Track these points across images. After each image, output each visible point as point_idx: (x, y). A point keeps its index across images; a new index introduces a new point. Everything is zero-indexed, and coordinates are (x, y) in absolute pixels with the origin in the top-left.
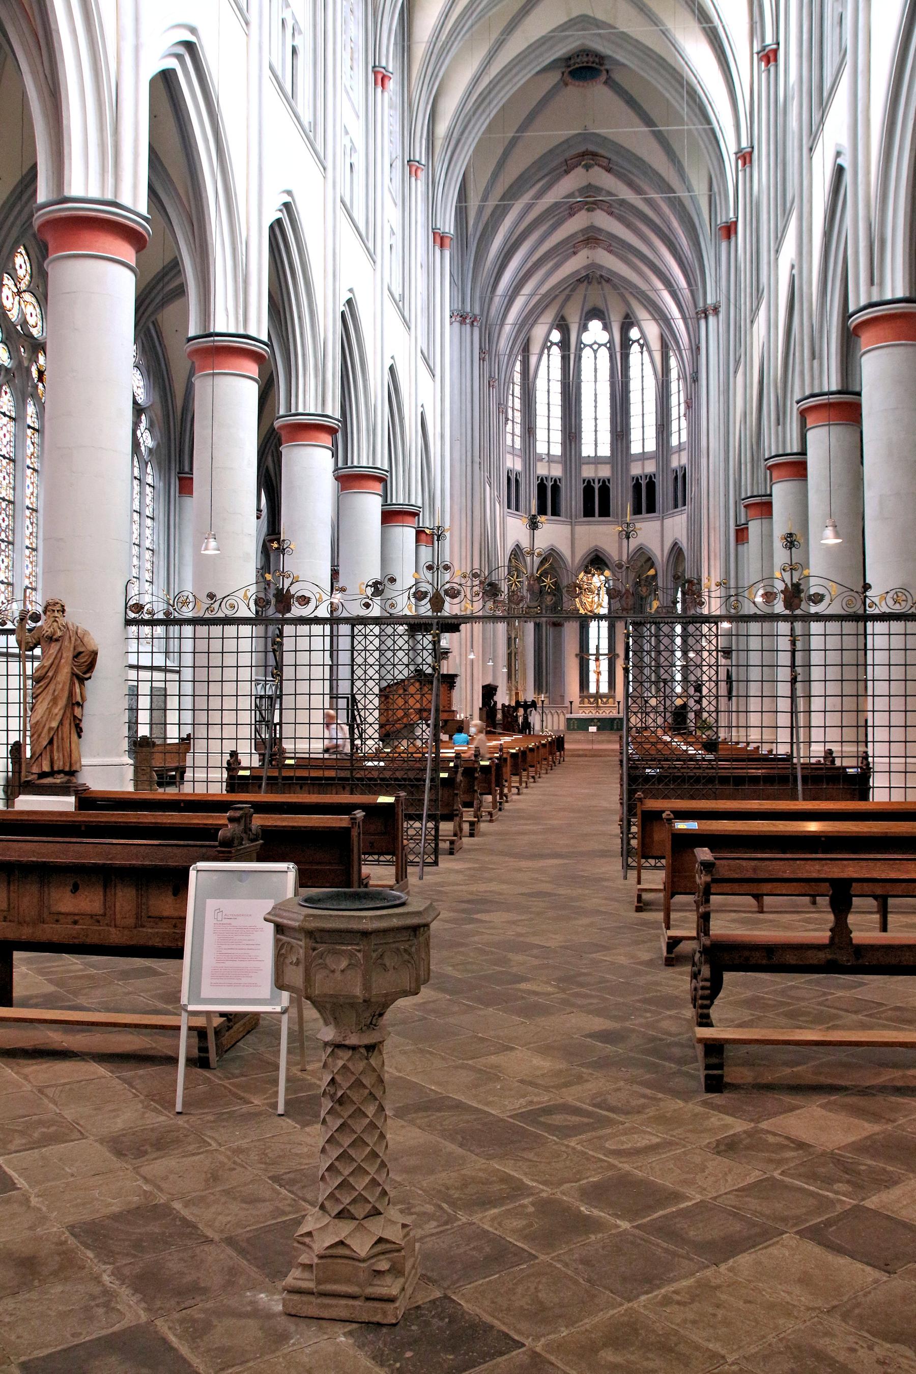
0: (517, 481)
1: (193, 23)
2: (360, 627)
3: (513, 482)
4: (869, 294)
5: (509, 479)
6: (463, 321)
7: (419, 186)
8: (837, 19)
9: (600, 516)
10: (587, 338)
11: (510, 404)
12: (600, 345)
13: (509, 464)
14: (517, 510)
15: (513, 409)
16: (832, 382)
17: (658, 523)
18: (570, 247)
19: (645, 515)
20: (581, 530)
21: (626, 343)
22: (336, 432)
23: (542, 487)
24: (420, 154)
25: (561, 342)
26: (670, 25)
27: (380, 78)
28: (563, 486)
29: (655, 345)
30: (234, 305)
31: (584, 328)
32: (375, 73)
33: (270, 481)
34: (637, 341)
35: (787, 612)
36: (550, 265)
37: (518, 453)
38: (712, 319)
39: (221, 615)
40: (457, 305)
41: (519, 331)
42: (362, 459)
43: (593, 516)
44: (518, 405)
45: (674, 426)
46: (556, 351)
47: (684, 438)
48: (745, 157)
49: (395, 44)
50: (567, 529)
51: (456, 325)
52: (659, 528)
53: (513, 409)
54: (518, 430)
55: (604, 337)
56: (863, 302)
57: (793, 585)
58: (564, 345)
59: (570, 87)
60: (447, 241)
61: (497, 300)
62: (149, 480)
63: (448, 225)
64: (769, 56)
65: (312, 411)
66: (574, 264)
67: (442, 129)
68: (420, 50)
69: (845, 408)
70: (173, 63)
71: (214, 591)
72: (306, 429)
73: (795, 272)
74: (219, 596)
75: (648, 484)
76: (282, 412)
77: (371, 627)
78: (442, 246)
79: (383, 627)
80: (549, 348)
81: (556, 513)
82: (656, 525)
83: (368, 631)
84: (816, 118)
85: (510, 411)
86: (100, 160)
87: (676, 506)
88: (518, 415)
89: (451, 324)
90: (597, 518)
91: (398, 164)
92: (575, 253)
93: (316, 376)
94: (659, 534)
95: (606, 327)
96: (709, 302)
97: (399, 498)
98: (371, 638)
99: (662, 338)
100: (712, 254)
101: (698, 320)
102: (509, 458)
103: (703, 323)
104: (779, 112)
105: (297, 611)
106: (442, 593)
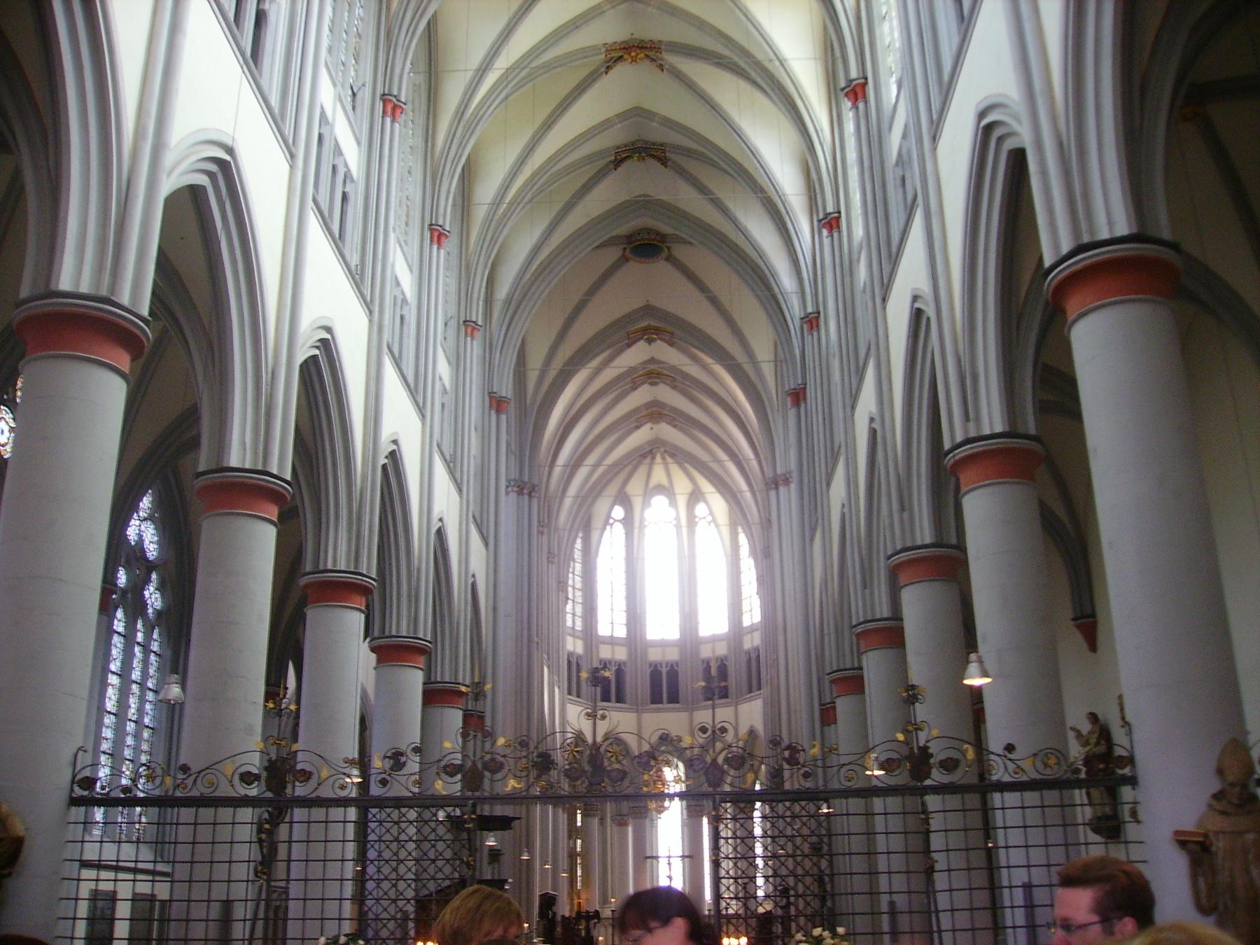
0: (578, 665)
1: (229, 142)
2: (374, 811)
3: (574, 664)
4: (966, 430)
5: (569, 662)
6: (520, 493)
7: (475, 349)
8: (899, 182)
9: (670, 701)
11: (570, 582)
15: (574, 588)
16: (925, 533)
21: (692, 521)
22: (368, 594)
24: (477, 315)
27: (437, 235)
30: (253, 436)
31: (646, 503)
32: (432, 230)
33: (287, 645)
35: (913, 783)
37: (580, 634)
38: (782, 489)
39: (195, 793)
40: (514, 474)
41: (580, 506)
42: (400, 627)
43: (661, 702)
44: (579, 585)
45: (745, 607)
48: (812, 321)
49: (454, 205)
51: (513, 496)
53: (574, 588)
54: (579, 610)
56: (959, 438)
57: (919, 748)
58: (628, 522)
59: (631, 263)
61: (557, 470)
62: (155, 646)
63: (506, 388)
64: (831, 223)
65: (343, 568)
67: (502, 292)
68: (480, 213)
69: (946, 563)
70: (203, 180)
71: (190, 764)
72: (339, 590)
73: (876, 426)
74: (194, 769)
76: (308, 568)
77: (388, 810)
78: (498, 412)
79: (404, 810)
81: (619, 700)
83: (384, 815)
84: (886, 269)
85: (570, 589)
86: (100, 253)
87: (750, 691)
88: (579, 594)
89: (507, 493)
91: (453, 323)
92: (638, 428)
93: (349, 531)
96: (779, 472)
97: (444, 674)
98: (388, 825)
100: (780, 427)
102: (569, 640)
103: (773, 494)
104: (846, 270)
105: (301, 790)
106: (479, 765)
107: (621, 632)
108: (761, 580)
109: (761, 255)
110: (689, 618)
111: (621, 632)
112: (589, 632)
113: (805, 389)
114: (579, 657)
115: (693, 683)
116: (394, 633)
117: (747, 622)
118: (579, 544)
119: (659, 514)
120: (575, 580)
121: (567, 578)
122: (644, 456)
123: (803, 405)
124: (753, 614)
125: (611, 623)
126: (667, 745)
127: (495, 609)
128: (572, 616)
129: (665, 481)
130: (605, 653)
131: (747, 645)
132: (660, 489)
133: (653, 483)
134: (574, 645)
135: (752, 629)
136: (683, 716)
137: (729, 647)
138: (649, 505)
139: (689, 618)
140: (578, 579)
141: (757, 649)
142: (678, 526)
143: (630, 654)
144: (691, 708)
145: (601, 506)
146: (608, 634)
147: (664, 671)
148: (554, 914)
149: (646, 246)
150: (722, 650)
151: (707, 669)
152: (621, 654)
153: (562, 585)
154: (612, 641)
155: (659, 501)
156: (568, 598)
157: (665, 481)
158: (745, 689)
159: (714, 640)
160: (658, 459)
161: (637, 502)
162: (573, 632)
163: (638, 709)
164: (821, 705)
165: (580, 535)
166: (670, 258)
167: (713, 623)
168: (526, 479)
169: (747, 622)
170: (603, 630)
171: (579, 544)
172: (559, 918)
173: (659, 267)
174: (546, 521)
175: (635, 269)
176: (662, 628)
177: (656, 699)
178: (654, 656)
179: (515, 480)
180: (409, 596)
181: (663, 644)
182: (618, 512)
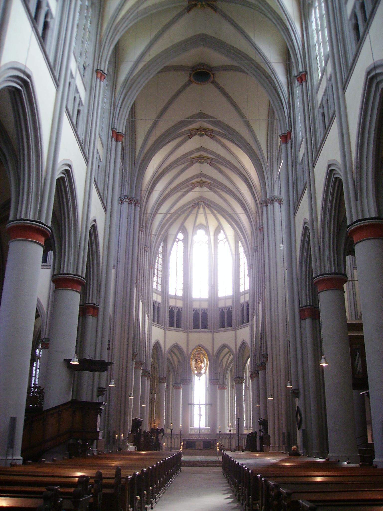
0: (158, 308)
5: (154, 306)
9: (202, 328)
10: (195, 238)
11: (156, 267)
13: (155, 298)
14: (158, 323)
17: (234, 332)
18: (189, 185)
21: (216, 241)
25: (183, 239)
26: (251, 35)
28: (183, 312)
29: (231, 239)
34: (222, 240)
36: (179, 194)
37: (160, 293)
44: (160, 269)
45: (242, 282)
46: (181, 244)
47: (247, 288)
51: (126, 204)
52: (234, 335)
53: (158, 270)
54: (160, 281)
55: (206, 237)
58: (185, 241)
59: (193, 84)
60: (120, 137)
75: (227, 312)
78: (117, 140)
80: (177, 242)
81: (178, 326)
82: (233, 333)
85: (156, 270)
87: (243, 323)
88: (160, 273)
94: (234, 338)
95: (208, 232)
97: (69, 268)
99: (236, 234)
101: (262, 207)
107: (180, 294)
108: (251, 267)
109: (267, 63)
110: (214, 288)
111: (180, 294)
112: (164, 293)
113: (290, 133)
114: (159, 304)
115: (214, 319)
116: (23, 217)
117: (242, 290)
118: (161, 249)
119: (200, 238)
120: (158, 266)
121: (154, 265)
122: (194, 206)
123: (289, 141)
124: (245, 285)
125: (175, 288)
126: (200, 349)
127: (109, 248)
128: (156, 283)
129: (204, 222)
130: (172, 303)
131: (242, 301)
132: (201, 226)
133: (198, 222)
135: (245, 293)
136: (210, 335)
137: (233, 303)
138: (196, 233)
139: (214, 288)
140: (160, 266)
141: (247, 303)
142: (209, 244)
143: (184, 304)
144: (213, 332)
145: (173, 230)
147: (201, 313)
148: (141, 430)
149: (202, 74)
150: (229, 303)
151: (222, 313)
152: (180, 304)
153: (151, 266)
154: (175, 298)
155: (201, 233)
156: (154, 274)
157: (204, 222)
158: (240, 321)
159: (226, 298)
160: (201, 211)
161: (190, 231)
162: (156, 292)
163: (187, 331)
165: (162, 244)
166: (214, 82)
167: (225, 291)
168: (134, 196)
169: (242, 290)
170: (171, 292)
171: (161, 249)
172: (142, 433)
173: (208, 88)
174: (144, 226)
175: (196, 88)
176: (200, 292)
177: (196, 326)
178: (196, 306)
179: (127, 196)
180: (37, 194)
181: (200, 300)
182: (180, 236)
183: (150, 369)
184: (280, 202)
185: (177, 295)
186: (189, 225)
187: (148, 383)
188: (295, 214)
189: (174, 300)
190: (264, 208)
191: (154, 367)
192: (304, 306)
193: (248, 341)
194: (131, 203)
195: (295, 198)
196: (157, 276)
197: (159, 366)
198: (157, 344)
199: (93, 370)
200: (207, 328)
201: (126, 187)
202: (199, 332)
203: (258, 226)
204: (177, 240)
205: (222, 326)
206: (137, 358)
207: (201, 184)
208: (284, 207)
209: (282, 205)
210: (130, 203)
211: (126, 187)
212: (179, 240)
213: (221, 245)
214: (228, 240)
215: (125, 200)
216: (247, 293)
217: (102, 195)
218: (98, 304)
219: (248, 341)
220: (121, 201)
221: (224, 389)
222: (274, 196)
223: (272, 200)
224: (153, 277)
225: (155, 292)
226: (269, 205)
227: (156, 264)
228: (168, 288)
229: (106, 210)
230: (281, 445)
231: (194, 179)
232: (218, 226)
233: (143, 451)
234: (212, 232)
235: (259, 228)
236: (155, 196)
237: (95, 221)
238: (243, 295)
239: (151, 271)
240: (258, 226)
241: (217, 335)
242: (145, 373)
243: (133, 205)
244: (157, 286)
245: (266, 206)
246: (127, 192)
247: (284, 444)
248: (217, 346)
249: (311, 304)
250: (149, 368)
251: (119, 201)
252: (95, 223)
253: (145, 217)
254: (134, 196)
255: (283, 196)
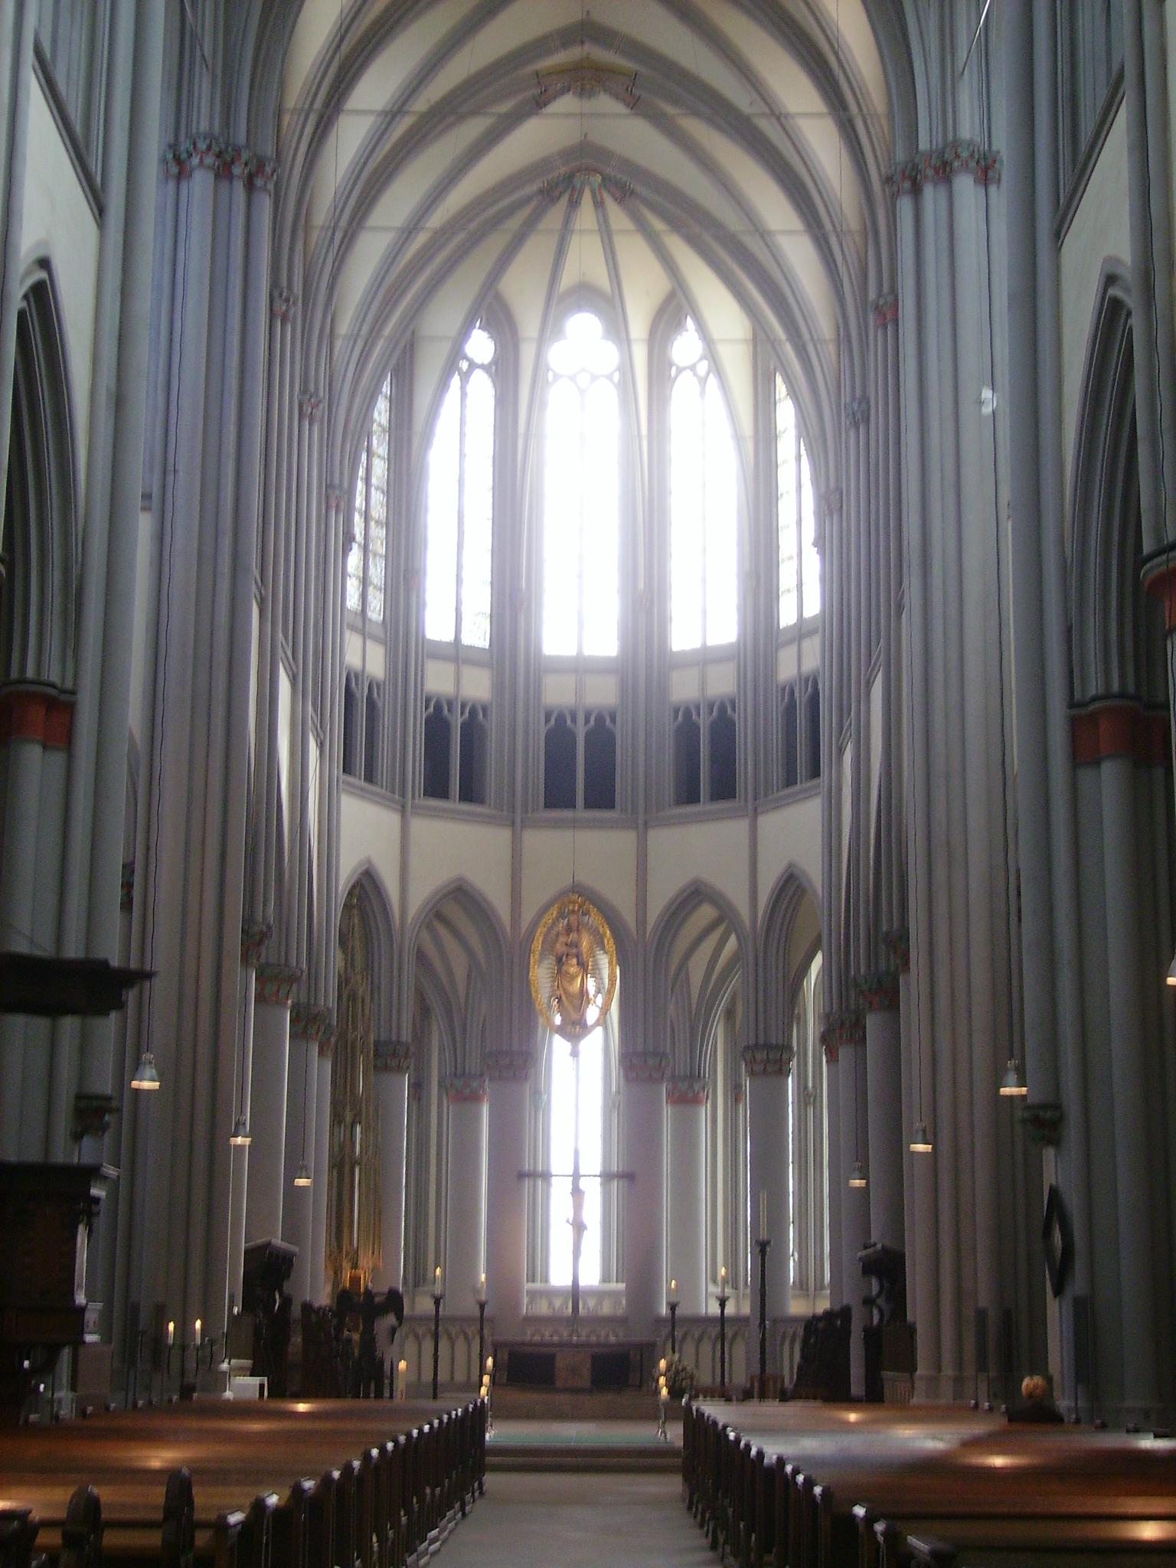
9: (589, 805)
10: (558, 355)
11: (359, 501)
12: (594, 378)
13: (352, 658)
14: (370, 778)
19: (705, 806)
20: (535, 840)
23: (437, 726)
25: (495, 361)
29: (737, 361)
36: (472, 129)
37: (379, 632)
43: (571, 804)
44: (378, 511)
46: (482, 387)
47: (813, 607)
50: (501, 837)
51: (201, 182)
55: (609, 354)
66: (535, 139)
80: (465, 377)
81: (471, 793)
82: (735, 830)
85: (358, 521)
87: (790, 780)
88: (378, 533)
90: (581, 813)
94: (745, 853)
99: (760, 341)
101: (894, 197)
107: (477, 635)
108: (831, 504)
110: (646, 603)
111: (477, 635)
115: (647, 759)
117: (787, 617)
118: (381, 412)
119: (581, 353)
120: (370, 497)
122: (549, 195)
124: (803, 592)
125: (454, 608)
127: (119, 402)
128: (359, 582)
129: (600, 276)
130: (438, 681)
131: (787, 669)
132: (585, 295)
134: (363, 656)
135: (802, 631)
138: (558, 332)
139: (646, 603)
140: (377, 497)
141: (812, 682)
143: (498, 686)
144: (642, 824)
145: (442, 317)
146: (448, 636)
148: (287, 1301)
150: (723, 684)
152: (477, 687)
153: (336, 497)
154: (456, 654)
155: (583, 327)
156: (349, 538)
158: (777, 772)
159: (705, 658)
160: (586, 216)
161: (529, 324)
163: (514, 819)
164: (1072, 704)
165: (386, 388)
167: (705, 619)
168: (241, 138)
169: (787, 617)
170: (437, 627)
171: (381, 412)
172: (296, 1311)
174: (295, 293)
176: (579, 627)
177: (558, 796)
178: (557, 694)
179: (210, 136)
181: (580, 668)
182: (480, 346)
183: (332, 1001)
184: (986, 171)
185: (466, 640)
186: (523, 287)
187: (321, 1071)
188: (1058, 236)
189: (450, 668)
190: (905, 205)
191: (353, 997)
192: (1094, 699)
193: (814, 871)
194: (230, 177)
195: (1065, 152)
196: (365, 549)
197: (375, 989)
198: (367, 885)
199: (53, 1010)
200: (611, 805)
201: (204, 89)
202: (574, 825)
203: (872, 295)
204: (464, 365)
205: (688, 794)
206: (269, 952)
207: (586, 78)
208: (1002, 197)
209: (993, 189)
210: (223, 172)
211: (204, 89)
212: (473, 366)
213: (684, 392)
214: (717, 368)
215: (195, 161)
216: (812, 633)
217: (78, 129)
218: (69, 685)
219: (814, 871)
220: (178, 166)
221: (696, 1100)
222: (956, 144)
223: (945, 164)
224: (346, 550)
225: (353, 628)
226: (928, 191)
227: (360, 486)
228: (421, 606)
229: (100, 210)
230: (970, 1371)
231: (549, 52)
232: (671, 297)
233: (299, 1397)
234: (638, 326)
235: (877, 308)
236: (350, 137)
237: (44, 263)
238: (790, 642)
239: (335, 521)
240: (872, 295)
241: (661, 839)
242: (306, 1022)
243: (239, 187)
244: (364, 597)
245: (916, 191)
246: (205, 119)
247: (982, 1365)
248: (662, 894)
249: (1131, 689)
250: (329, 998)
251: (164, 161)
252: (42, 275)
253: (299, 247)
254: (241, 138)
255: (1003, 142)
